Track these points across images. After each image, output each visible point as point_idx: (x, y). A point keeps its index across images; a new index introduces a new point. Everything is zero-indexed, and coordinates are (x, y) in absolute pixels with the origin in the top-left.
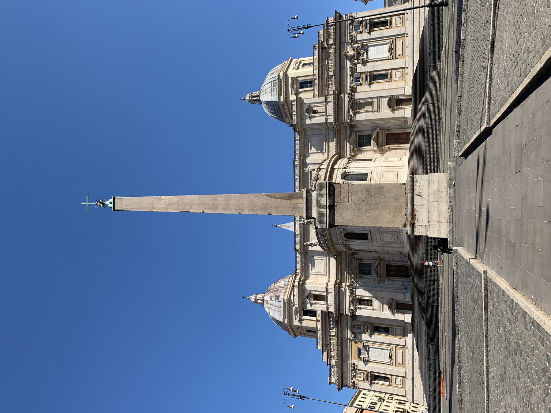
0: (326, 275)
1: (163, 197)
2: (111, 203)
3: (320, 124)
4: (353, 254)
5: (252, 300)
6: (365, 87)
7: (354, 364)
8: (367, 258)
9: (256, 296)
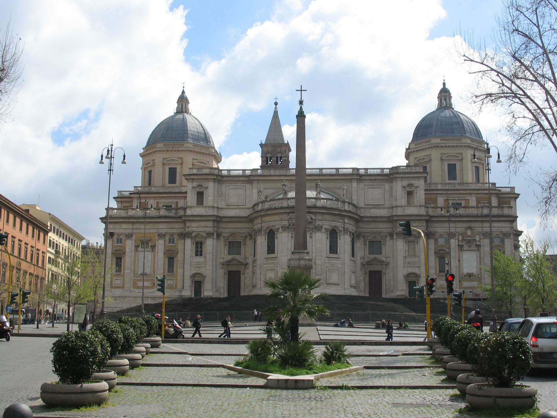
3: (396, 200)
4: (250, 235)
6: (432, 247)
7: (131, 235)
8: (246, 250)
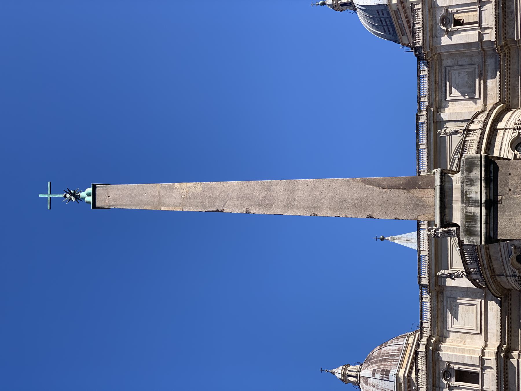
0: (480, 334)
1: (177, 185)
2: (89, 195)
3: (469, 44)
5: (339, 376)
9: (346, 369)
